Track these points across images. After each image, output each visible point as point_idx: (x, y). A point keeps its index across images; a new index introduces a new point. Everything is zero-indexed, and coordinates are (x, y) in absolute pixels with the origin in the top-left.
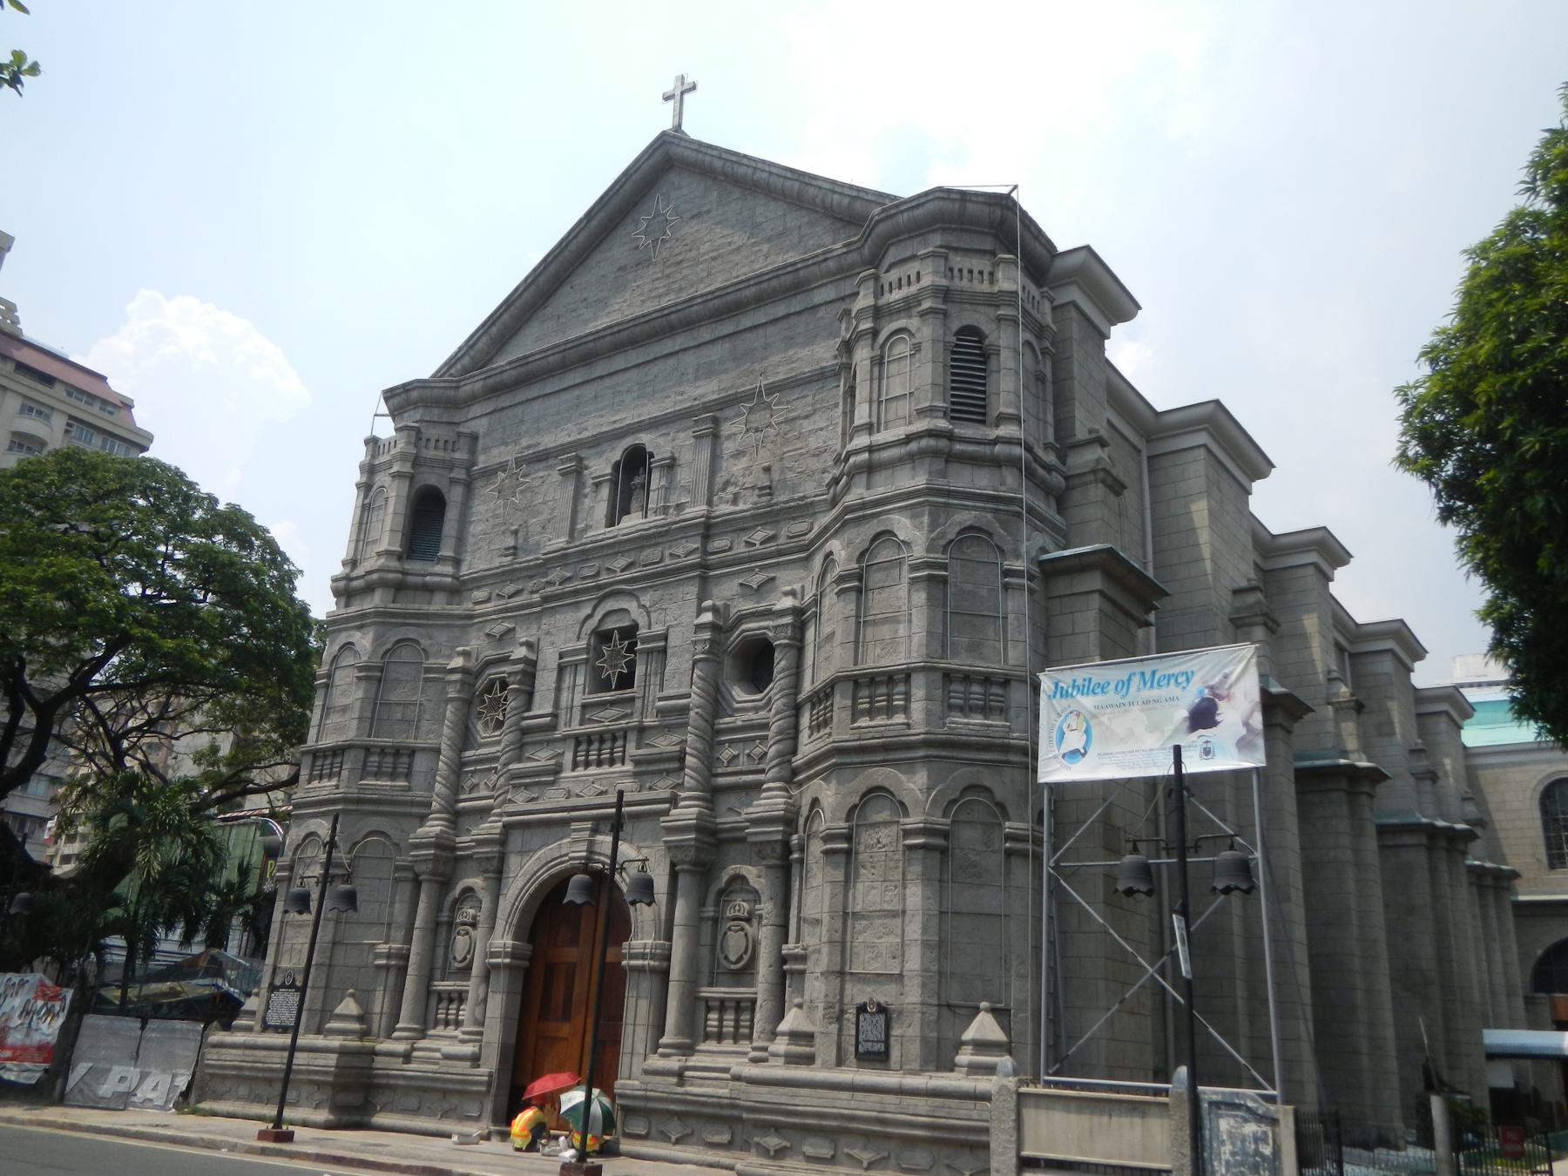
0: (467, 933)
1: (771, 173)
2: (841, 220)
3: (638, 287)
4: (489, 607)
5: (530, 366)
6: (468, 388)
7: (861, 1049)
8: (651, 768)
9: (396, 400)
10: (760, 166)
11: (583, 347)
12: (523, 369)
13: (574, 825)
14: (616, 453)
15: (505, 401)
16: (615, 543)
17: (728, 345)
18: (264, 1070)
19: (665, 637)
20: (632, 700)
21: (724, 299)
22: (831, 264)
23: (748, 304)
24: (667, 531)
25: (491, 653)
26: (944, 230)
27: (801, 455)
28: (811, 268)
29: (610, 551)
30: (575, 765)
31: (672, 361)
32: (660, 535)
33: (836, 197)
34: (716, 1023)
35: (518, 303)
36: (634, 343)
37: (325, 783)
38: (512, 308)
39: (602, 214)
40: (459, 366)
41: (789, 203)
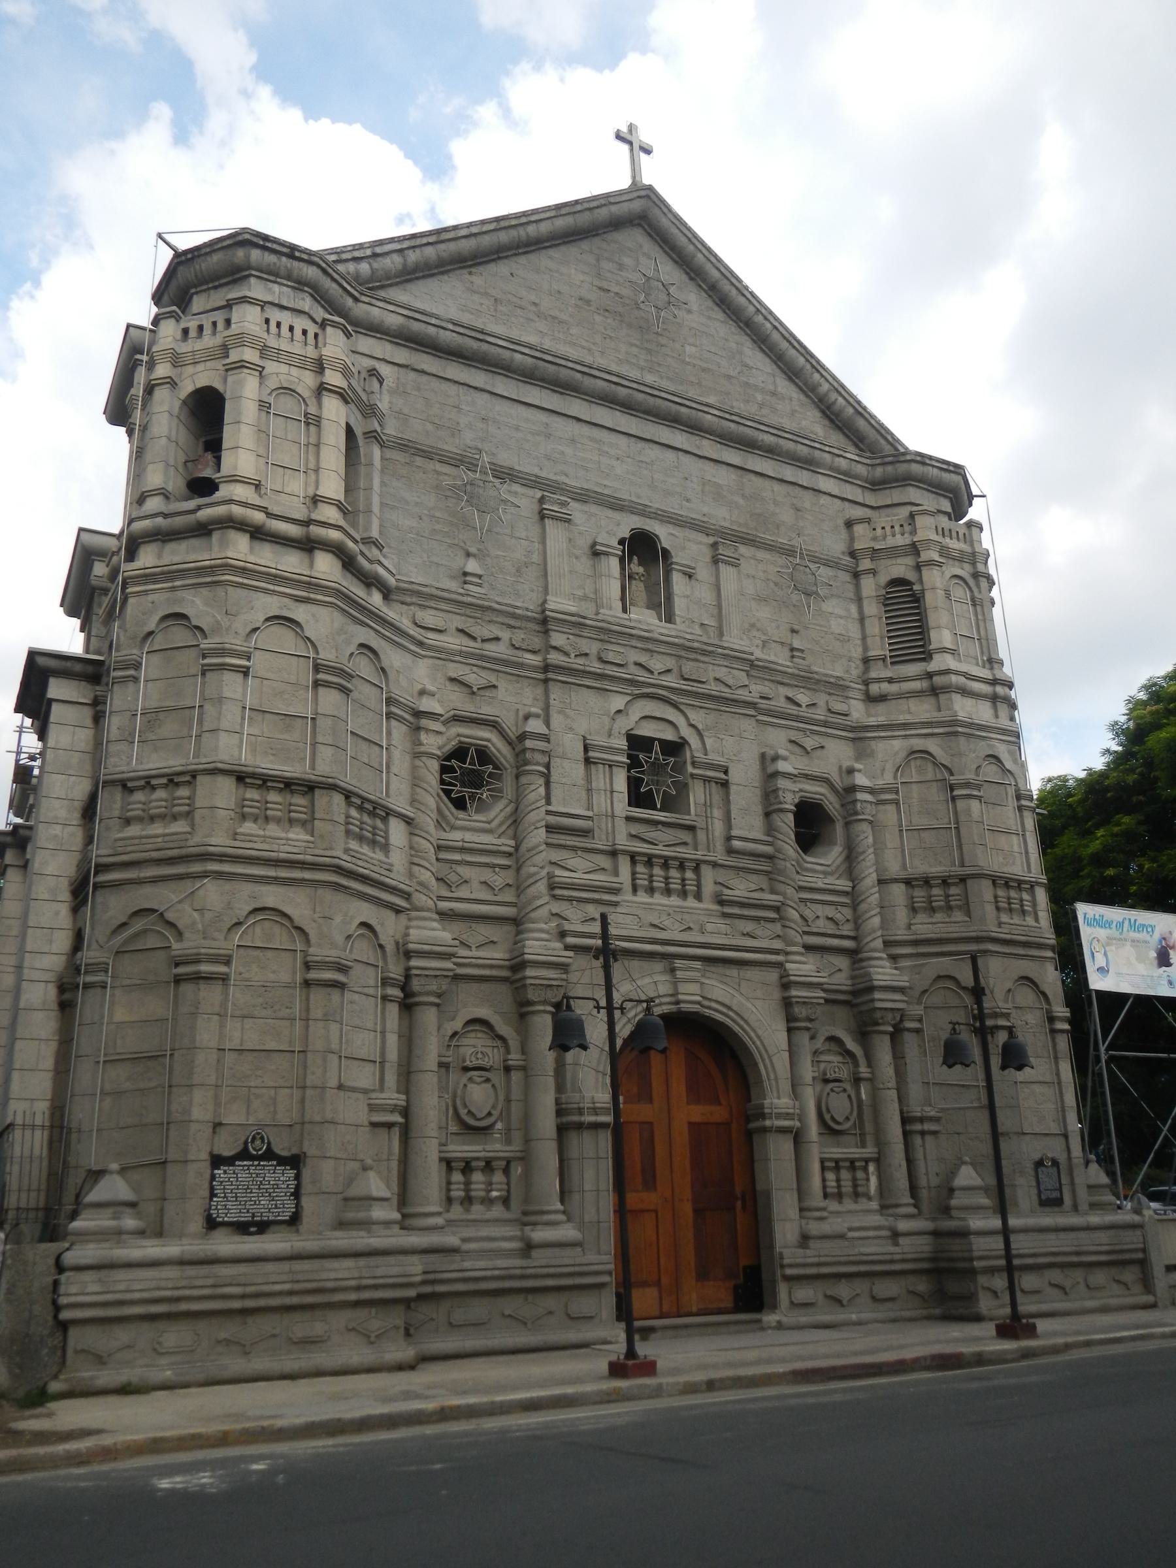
0: (488, 1080)
1: (775, 327)
2: (832, 421)
3: (611, 338)
4: (453, 642)
5: (485, 347)
6: (375, 312)
7: (1043, 1197)
8: (746, 912)
9: (271, 259)
10: (763, 311)
11: (563, 371)
12: (475, 345)
13: (678, 963)
14: (626, 525)
15: (426, 362)
16: (647, 638)
17: (733, 477)
18: (243, 1296)
19: (726, 772)
20: (691, 828)
21: (742, 428)
22: (843, 464)
23: (759, 448)
24: (712, 652)
25: (457, 701)
26: (951, 499)
27: (826, 633)
28: (827, 456)
29: (639, 645)
30: (635, 889)
31: (670, 455)
32: (705, 653)
33: (840, 400)
34: (834, 1184)
35: (452, 246)
36: (627, 407)
37: (273, 830)
38: (442, 247)
39: (569, 220)
40: (351, 267)
41: (780, 368)
